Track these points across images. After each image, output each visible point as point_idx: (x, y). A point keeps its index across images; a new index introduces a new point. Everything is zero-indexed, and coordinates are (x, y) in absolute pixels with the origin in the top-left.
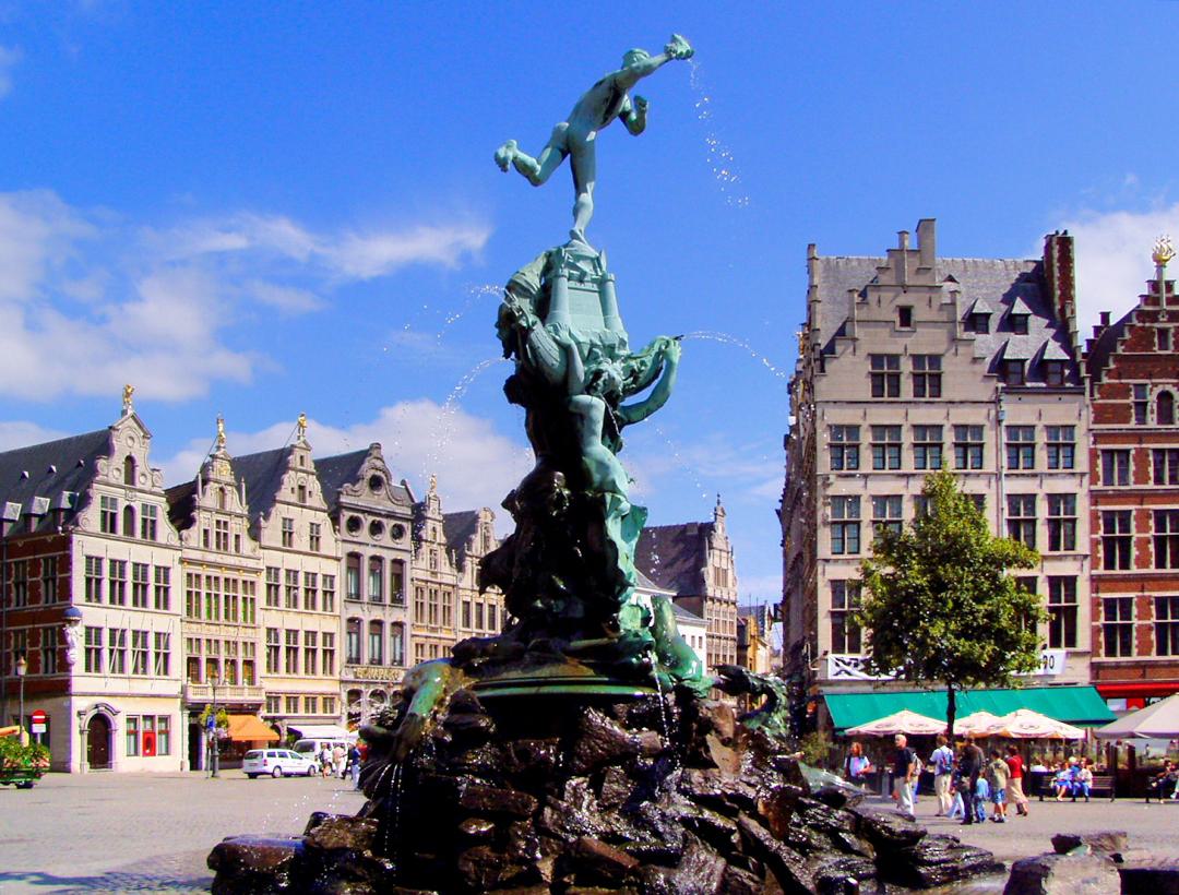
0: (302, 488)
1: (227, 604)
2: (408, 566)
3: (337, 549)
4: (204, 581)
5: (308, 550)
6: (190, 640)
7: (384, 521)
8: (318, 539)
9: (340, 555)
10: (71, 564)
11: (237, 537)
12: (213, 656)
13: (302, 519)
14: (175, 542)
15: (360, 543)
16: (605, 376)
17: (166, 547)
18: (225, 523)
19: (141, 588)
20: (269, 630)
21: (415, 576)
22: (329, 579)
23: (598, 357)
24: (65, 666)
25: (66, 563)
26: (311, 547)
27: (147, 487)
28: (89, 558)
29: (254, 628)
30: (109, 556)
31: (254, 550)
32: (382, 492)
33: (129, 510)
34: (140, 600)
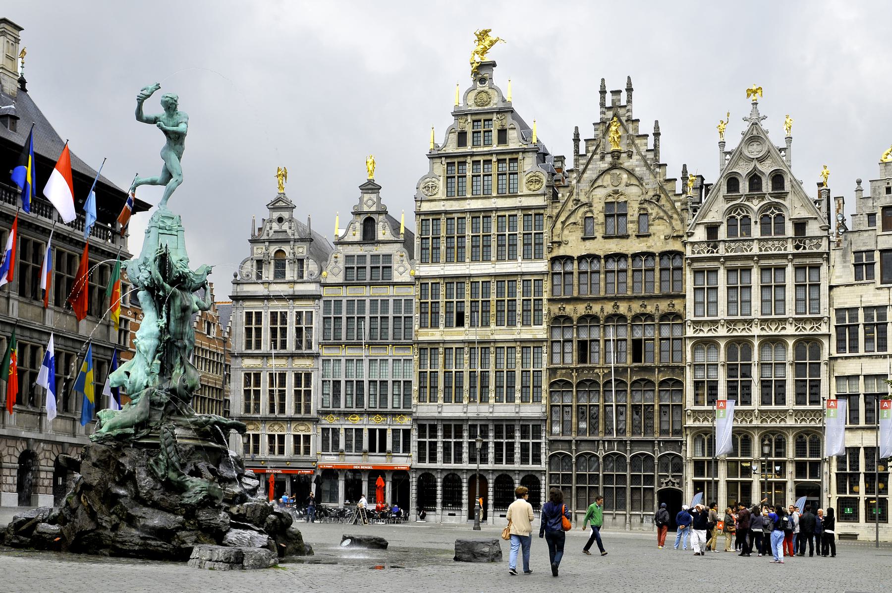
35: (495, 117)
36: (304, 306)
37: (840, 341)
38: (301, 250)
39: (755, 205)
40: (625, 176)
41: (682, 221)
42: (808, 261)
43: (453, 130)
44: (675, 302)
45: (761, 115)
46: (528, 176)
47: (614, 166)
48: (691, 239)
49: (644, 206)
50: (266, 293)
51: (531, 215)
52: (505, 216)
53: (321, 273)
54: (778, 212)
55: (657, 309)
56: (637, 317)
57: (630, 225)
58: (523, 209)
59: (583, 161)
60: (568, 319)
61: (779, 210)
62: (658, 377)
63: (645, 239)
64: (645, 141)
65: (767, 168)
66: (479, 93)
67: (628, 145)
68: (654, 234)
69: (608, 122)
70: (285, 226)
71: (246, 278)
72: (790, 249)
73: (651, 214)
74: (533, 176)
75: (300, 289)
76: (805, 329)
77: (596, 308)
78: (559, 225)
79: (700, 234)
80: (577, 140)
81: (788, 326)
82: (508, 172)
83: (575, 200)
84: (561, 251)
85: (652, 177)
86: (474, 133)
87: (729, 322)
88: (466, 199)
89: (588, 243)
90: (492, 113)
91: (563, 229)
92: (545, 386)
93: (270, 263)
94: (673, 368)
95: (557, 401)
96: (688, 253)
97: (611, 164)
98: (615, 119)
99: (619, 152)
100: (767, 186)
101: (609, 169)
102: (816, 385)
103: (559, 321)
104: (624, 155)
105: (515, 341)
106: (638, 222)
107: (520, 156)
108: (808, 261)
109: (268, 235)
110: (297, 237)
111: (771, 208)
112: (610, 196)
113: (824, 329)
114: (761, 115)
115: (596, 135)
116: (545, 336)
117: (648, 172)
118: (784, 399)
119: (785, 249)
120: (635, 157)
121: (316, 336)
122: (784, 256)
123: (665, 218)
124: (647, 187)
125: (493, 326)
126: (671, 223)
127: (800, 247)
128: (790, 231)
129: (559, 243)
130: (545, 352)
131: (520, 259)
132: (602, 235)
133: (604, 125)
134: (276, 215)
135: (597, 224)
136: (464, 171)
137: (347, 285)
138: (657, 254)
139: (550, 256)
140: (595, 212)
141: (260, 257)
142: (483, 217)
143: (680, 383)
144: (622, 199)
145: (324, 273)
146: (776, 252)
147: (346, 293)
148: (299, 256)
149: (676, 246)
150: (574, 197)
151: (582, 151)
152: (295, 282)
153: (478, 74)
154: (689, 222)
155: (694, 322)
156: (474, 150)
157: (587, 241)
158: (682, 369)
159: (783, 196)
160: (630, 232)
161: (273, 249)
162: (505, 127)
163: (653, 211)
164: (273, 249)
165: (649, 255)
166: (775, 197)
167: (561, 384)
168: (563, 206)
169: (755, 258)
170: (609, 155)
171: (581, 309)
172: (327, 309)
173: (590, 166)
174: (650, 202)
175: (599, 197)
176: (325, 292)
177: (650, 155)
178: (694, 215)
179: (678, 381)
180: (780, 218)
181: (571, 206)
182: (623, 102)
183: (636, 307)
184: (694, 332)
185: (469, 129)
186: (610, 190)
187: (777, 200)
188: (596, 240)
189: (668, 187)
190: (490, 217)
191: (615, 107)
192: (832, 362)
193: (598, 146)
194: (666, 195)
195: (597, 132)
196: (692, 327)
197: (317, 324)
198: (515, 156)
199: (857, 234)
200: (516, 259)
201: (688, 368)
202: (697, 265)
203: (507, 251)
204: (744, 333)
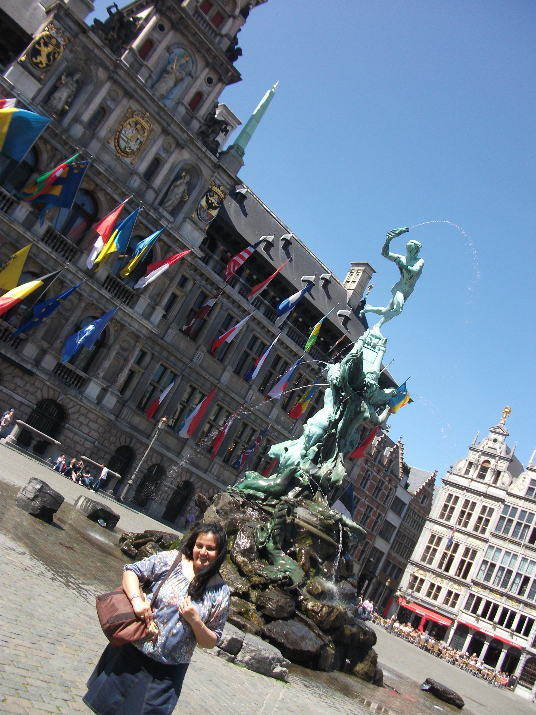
36: (490, 504)
38: (502, 465)
50: (467, 485)
53: (510, 485)
70: (497, 446)
71: (458, 471)
75: (492, 491)
93: (477, 466)
109: (483, 448)
110: (502, 455)
121: (491, 527)
134: (493, 436)
137: (526, 499)
141: (473, 461)
145: (512, 485)
147: (522, 505)
148: (499, 468)
152: (489, 485)
161: (483, 458)
164: (483, 458)
172: (505, 511)
176: (509, 500)
197: (494, 519)
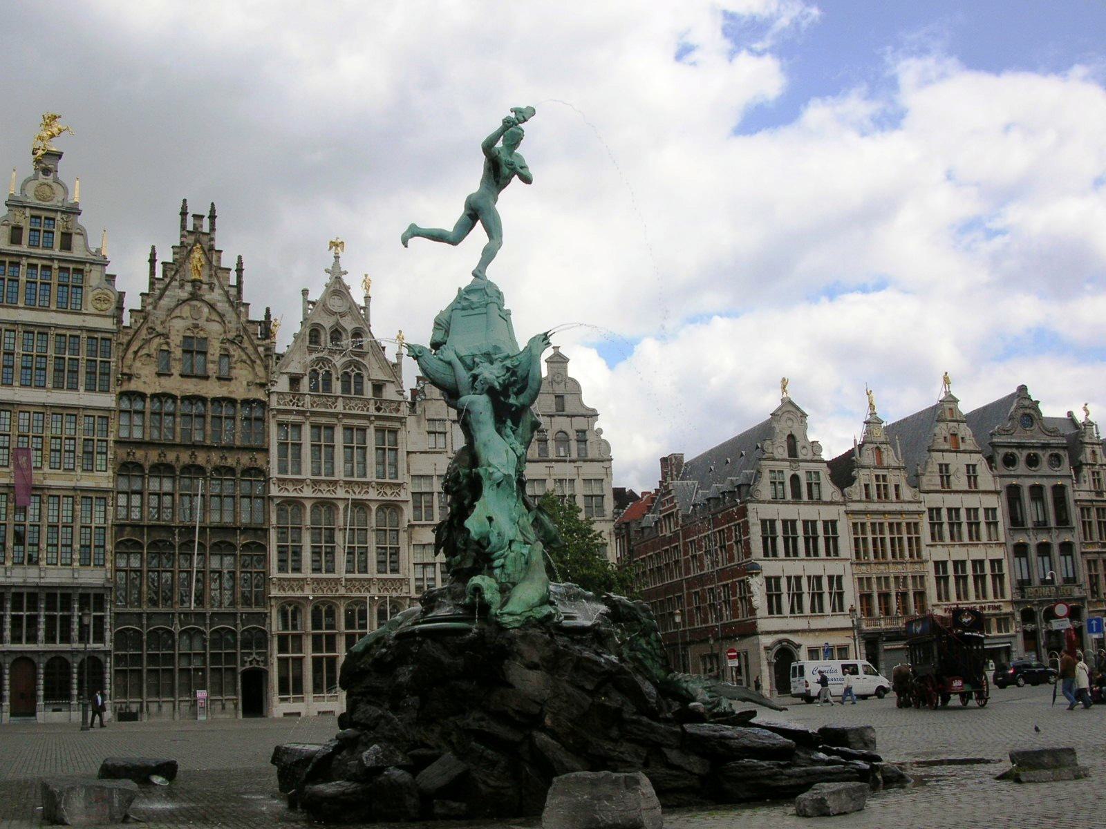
0: (954, 435)
1: (893, 545)
2: (1069, 491)
3: (995, 483)
4: (869, 529)
5: (967, 488)
6: (860, 579)
7: (1040, 453)
8: (975, 477)
9: (999, 488)
10: (748, 528)
11: (897, 487)
12: (902, 589)
13: (958, 463)
14: (838, 498)
15: (1018, 476)
16: (480, 378)
17: (832, 503)
18: (884, 476)
19: (811, 540)
20: (937, 563)
21: (1078, 498)
22: (991, 511)
23: (478, 364)
24: (752, 611)
25: (745, 528)
26: (970, 486)
27: (809, 457)
28: (764, 522)
29: (922, 562)
30: (782, 517)
31: (915, 496)
32: (1035, 427)
33: (795, 479)
34: (812, 551)
35: (59, 216)
37: (417, 508)
39: (338, 361)
40: (206, 310)
41: (266, 367)
42: (388, 424)
43: (6, 222)
44: (259, 456)
45: (342, 270)
46: (95, 292)
47: (194, 296)
48: (273, 389)
49: (224, 346)
51: (97, 339)
52: (65, 335)
54: (357, 372)
55: (238, 463)
56: (217, 469)
57: (210, 366)
58: (89, 330)
59: (159, 285)
60: (139, 466)
61: (359, 369)
62: (241, 540)
63: (226, 382)
64: (225, 275)
65: (349, 324)
66: (41, 185)
67: (211, 276)
68: (236, 378)
69: (189, 248)
72: (372, 411)
73: (233, 356)
74: (103, 294)
76: (386, 494)
77: (171, 456)
78: (130, 355)
79: (283, 384)
80: (152, 261)
81: (371, 490)
82: (70, 284)
83: (151, 328)
84: (133, 386)
85: (234, 315)
86: (31, 230)
87: (315, 483)
88: (18, 308)
89: (163, 380)
90: (56, 211)
91: (134, 359)
92: (109, 547)
94: (255, 530)
95: (122, 563)
96: (274, 403)
97: (191, 294)
98: (198, 246)
99: (201, 282)
100: (347, 342)
101: (187, 300)
102: (396, 551)
103: (126, 469)
104: (205, 287)
105: (74, 489)
106: (220, 363)
107: (87, 267)
108: (388, 424)
111: (350, 366)
112: (189, 329)
113: (403, 497)
114: (342, 270)
115: (175, 260)
116: (111, 485)
117: (231, 309)
118: (366, 567)
119: (368, 410)
120: (218, 291)
122: (367, 417)
123: (248, 362)
124: (230, 325)
125: (46, 469)
126: (253, 368)
127: (381, 409)
128: (368, 391)
129: (130, 377)
130: (110, 504)
131: (82, 389)
132: (179, 372)
133: (183, 251)
135: (175, 360)
136: (16, 274)
138: (239, 401)
139: (118, 389)
140: (172, 345)
142: (39, 333)
143: (264, 548)
144: (202, 334)
146: (359, 412)
149: (260, 395)
150: (150, 325)
151: (159, 274)
153: (41, 162)
154: (274, 369)
155: (279, 480)
156: (32, 250)
157: (162, 377)
158: (266, 531)
159: (362, 355)
160: (210, 373)
162: (70, 231)
163: (236, 353)
165: (232, 402)
166: (355, 355)
167: (129, 544)
168: (136, 333)
169: (341, 416)
170: (190, 284)
171: (153, 456)
173: (167, 293)
174: (232, 342)
175: (178, 328)
177: (233, 292)
178: (277, 363)
179: (260, 545)
180: (359, 376)
181: (144, 334)
182: (206, 229)
183: (215, 457)
184: (280, 491)
185: (26, 226)
186: (189, 323)
187: (357, 358)
188: (172, 377)
189: (251, 328)
190: (47, 334)
191: (196, 231)
192: (410, 530)
193: (177, 271)
194: (249, 337)
195: (177, 256)
196: (276, 485)
198: (81, 267)
199: (430, 402)
200: (77, 389)
201: (272, 531)
202: (281, 417)
203: (65, 376)
204: (328, 495)
